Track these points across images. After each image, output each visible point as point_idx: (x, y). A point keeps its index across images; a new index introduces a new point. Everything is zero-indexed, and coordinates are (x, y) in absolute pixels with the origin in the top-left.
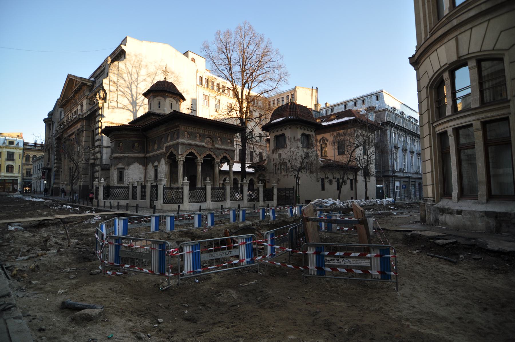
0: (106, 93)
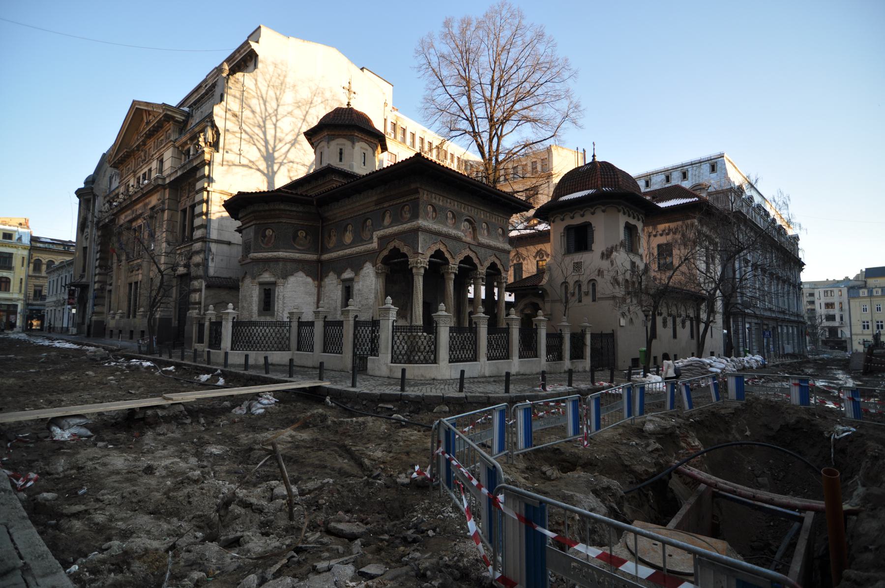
0: (218, 133)
